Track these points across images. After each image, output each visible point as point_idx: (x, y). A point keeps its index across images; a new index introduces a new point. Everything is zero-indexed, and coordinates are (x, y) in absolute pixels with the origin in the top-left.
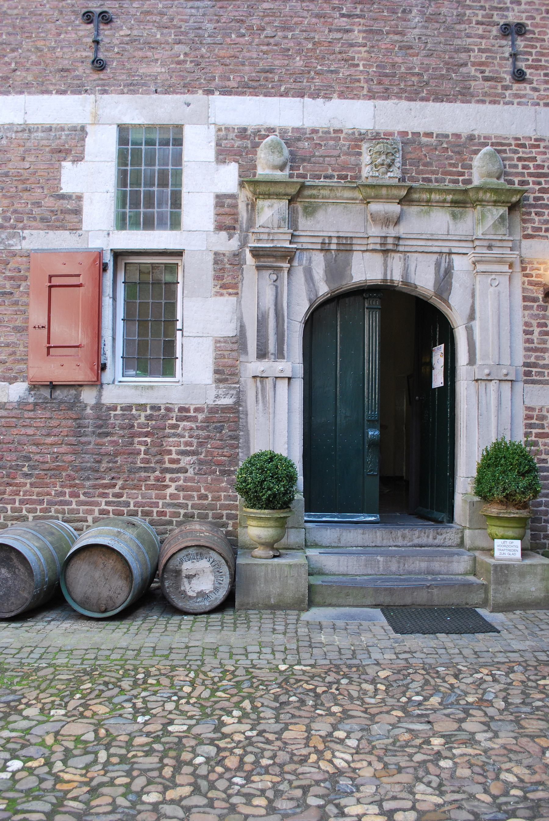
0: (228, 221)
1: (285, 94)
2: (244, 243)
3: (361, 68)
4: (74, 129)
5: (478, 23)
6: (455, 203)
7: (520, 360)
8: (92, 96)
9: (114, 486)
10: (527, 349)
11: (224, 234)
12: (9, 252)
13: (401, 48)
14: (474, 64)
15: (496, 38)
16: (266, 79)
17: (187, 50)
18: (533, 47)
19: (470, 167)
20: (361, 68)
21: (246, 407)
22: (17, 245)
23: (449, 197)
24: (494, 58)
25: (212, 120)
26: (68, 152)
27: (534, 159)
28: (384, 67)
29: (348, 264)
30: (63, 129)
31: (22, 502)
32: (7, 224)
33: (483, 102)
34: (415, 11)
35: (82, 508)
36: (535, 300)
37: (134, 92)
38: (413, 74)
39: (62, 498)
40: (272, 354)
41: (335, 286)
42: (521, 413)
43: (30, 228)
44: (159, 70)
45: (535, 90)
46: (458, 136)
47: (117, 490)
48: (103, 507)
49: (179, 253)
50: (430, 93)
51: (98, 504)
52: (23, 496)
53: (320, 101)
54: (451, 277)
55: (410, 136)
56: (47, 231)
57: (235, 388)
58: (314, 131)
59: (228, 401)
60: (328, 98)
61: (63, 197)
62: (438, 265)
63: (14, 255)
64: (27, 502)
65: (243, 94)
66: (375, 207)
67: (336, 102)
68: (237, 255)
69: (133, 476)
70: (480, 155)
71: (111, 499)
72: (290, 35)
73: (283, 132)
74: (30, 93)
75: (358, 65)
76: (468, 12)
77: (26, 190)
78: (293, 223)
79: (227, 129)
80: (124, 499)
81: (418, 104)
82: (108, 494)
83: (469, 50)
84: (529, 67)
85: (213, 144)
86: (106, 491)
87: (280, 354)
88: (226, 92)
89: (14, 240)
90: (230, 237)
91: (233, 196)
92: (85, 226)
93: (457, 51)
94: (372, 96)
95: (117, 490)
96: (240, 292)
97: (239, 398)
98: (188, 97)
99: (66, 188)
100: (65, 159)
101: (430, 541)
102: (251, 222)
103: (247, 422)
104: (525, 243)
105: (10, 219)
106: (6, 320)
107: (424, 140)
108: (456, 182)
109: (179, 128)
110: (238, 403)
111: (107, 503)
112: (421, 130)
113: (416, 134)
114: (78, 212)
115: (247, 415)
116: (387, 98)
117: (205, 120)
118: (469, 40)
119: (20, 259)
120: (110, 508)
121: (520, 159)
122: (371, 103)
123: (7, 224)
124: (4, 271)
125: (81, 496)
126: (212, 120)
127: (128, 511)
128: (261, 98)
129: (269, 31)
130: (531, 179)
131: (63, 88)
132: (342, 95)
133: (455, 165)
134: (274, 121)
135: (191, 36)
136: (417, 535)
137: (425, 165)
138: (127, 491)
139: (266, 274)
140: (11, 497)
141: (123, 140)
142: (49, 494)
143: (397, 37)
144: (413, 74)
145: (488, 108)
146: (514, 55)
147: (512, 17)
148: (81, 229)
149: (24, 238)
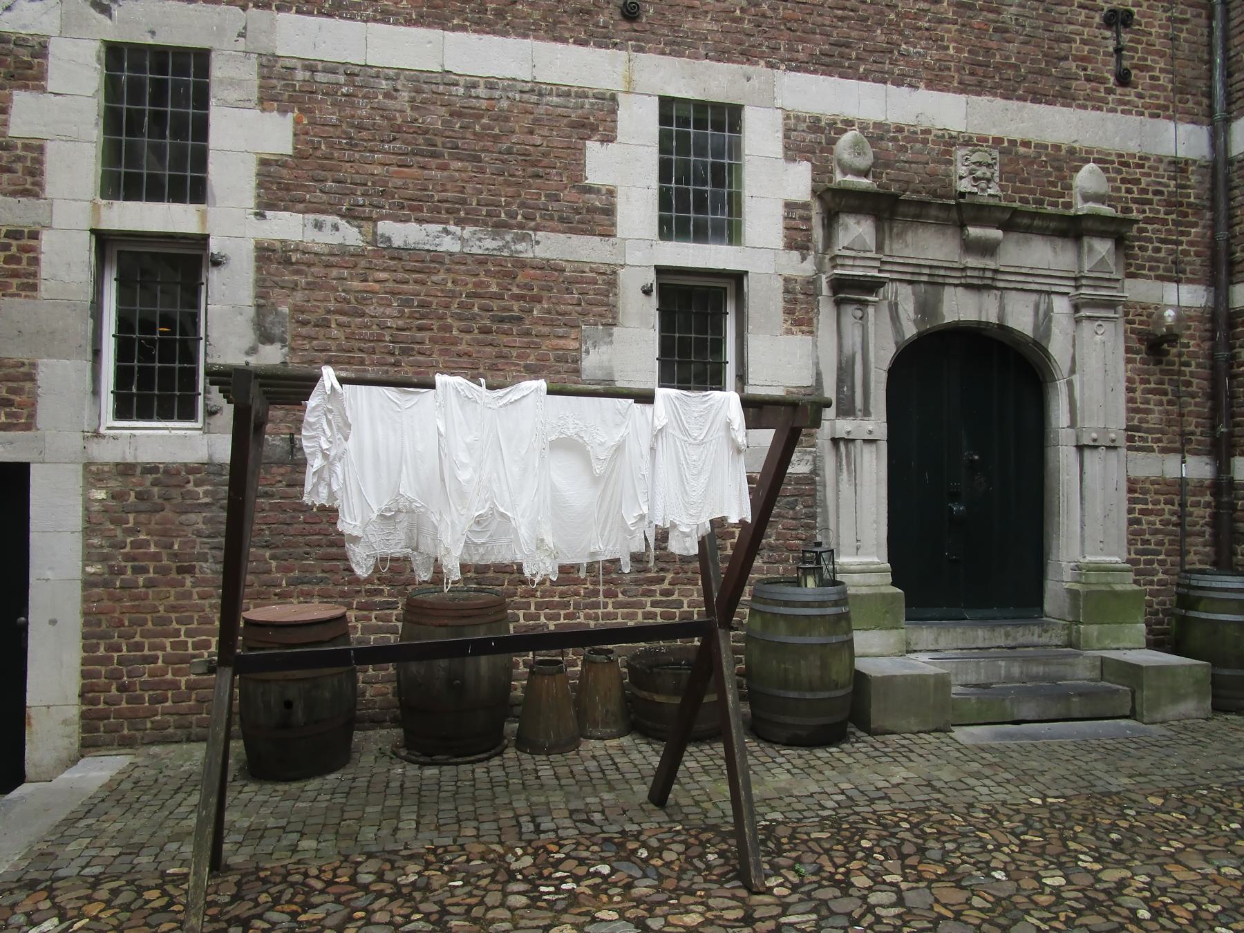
0: (799, 238)
1: (862, 78)
2: (820, 270)
3: (951, 52)
4: (600, 96)
8: (624, 53)
9: (662, 580)
10: (1129, 410)
11: (795, 255)
12: (516, 261)
13: (996, 30)
14: (1076, 59)
16: (842, 56)
18: (1139, 42)
19: (1070, 188)
20: (951, 52)
21: (824, 476)
22: (525, 251)
23: (1053, 225)
24: (1097, 53)
26: (594, 129)
27: (1138, 182)
28: (977, 54)
29: (939, 301)
31: (539, 606)
32: (513, 222)
33: (1085, 107)
35: (620, 611)
37: (680, 54)
39: (594, 599)
40: (860, 410)
41: (922, 329)
43: (544, 229)
44: (709, 27)
45: (1140, 96)
46: (1057, 147)
47: (666, 585)
48: (649, 609)
50: (1027, 91)
51: (642, 605)
52: (541, 597)
53: (905, 90)
54: (1050, 321)
55: (1006, 144)
56: (568, 235)
57: (811, 452)
58: (900, 129)
61: (589, 190)
62: (1037, 307)
63: (522, 264)
64: (549, 605)
66: (974, 231)
68: (812, 282)
69: (686, 567)
71: (659, 598)
73: (863, 127)
74: (536, 38)
75: (947, 48)
77: (538, 176)
79: (797, 118)
80: (675, 597)
81: (1014, 104)
82: (655, 591)
84: (1136, 67)
85: (780, 135)
86: (653, 588)
87: (867, 413)
88: (799, 67)
89: (524, 244)
90: (804, 259)
91: (806, 206)
92: (621, 231)
93: (1058, 40)
94: (963, 89)
95: (666, 585)
96: (815, 330)
97: (815, 464)
99: (593, 177)
100: (589, 138)
101: (1035, 639)
103: (825, 495)
104: (1128, 283)
105: (517, 214)
106: (515, 354)
107: (1022, 150)
108: (1055, 205)
110: (814, 472)
111: (654, 604)
112: (1017, 137)
113: (1013, 142)
114: (609, 211)
115: (825, 486)
117: (768, 102)
118: (1071, 27)
119: (532, 272)
120: (658, 610)
121: (1123, 181)
122: (963, 97)
123: (513, 222)
124: (509, 287)
125: (620, 595)
126: (778, 103)
127: (681, 613)
128: (836, 79)
130: (1134, 206)
131: (583, 36)
132: (930, 85)
133: (1054, 184)
134: (851, 112)
136: (1021, 633)
137: (1024, 181)
138: (678, 586)
140: (524, 600)
141: (664, 119)
142: (578, 594)
143: (991, 16)
145: (1090, 115)
146: (1118, 51)
148: (615, 236)
149: (538, 243)
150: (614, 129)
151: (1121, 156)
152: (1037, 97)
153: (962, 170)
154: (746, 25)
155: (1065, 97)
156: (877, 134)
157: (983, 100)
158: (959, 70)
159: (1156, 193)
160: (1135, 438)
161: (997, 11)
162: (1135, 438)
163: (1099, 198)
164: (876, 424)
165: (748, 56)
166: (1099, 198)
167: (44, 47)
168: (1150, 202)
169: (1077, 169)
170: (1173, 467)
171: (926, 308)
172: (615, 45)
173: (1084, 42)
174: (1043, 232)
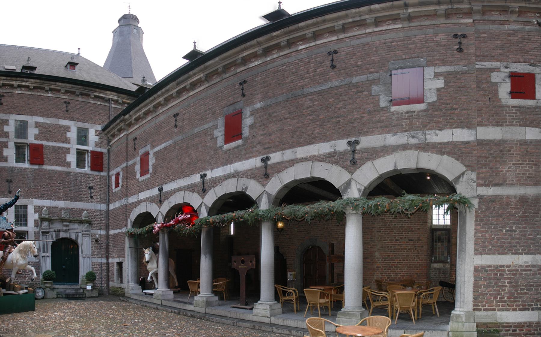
2: (40, 230)
6: (79, 223)
7: (91, 253)
29: (59, 234)
36: (93, 241)
42: (91, 263)
46: (80, 209)
49: (28, 231)
58: (53, 207)
59: (37, 261)
60: (55, 200)
62: (76, 234)
66: (64, 223)
67: (57, 201)
68: (39, 232)
73: (47, 207)
78: (49, 227)
91: (37, 220)
98: (28, 199)
102: (41, 226)
104: (92, 230)
109: (27, 206)
129: (44, 186)
139: (44, 236)
147: (91, 185)
153: (63, 214)
155: (81, 201)
156: (49, 208)
157: (67, 202)
160: (93, 255)
162: (93, 255)
163: (85, 217)
164: (49, 254)
166: (85, 217)
170: (100, 260)
171: (57, 235)
174: (77, 223)
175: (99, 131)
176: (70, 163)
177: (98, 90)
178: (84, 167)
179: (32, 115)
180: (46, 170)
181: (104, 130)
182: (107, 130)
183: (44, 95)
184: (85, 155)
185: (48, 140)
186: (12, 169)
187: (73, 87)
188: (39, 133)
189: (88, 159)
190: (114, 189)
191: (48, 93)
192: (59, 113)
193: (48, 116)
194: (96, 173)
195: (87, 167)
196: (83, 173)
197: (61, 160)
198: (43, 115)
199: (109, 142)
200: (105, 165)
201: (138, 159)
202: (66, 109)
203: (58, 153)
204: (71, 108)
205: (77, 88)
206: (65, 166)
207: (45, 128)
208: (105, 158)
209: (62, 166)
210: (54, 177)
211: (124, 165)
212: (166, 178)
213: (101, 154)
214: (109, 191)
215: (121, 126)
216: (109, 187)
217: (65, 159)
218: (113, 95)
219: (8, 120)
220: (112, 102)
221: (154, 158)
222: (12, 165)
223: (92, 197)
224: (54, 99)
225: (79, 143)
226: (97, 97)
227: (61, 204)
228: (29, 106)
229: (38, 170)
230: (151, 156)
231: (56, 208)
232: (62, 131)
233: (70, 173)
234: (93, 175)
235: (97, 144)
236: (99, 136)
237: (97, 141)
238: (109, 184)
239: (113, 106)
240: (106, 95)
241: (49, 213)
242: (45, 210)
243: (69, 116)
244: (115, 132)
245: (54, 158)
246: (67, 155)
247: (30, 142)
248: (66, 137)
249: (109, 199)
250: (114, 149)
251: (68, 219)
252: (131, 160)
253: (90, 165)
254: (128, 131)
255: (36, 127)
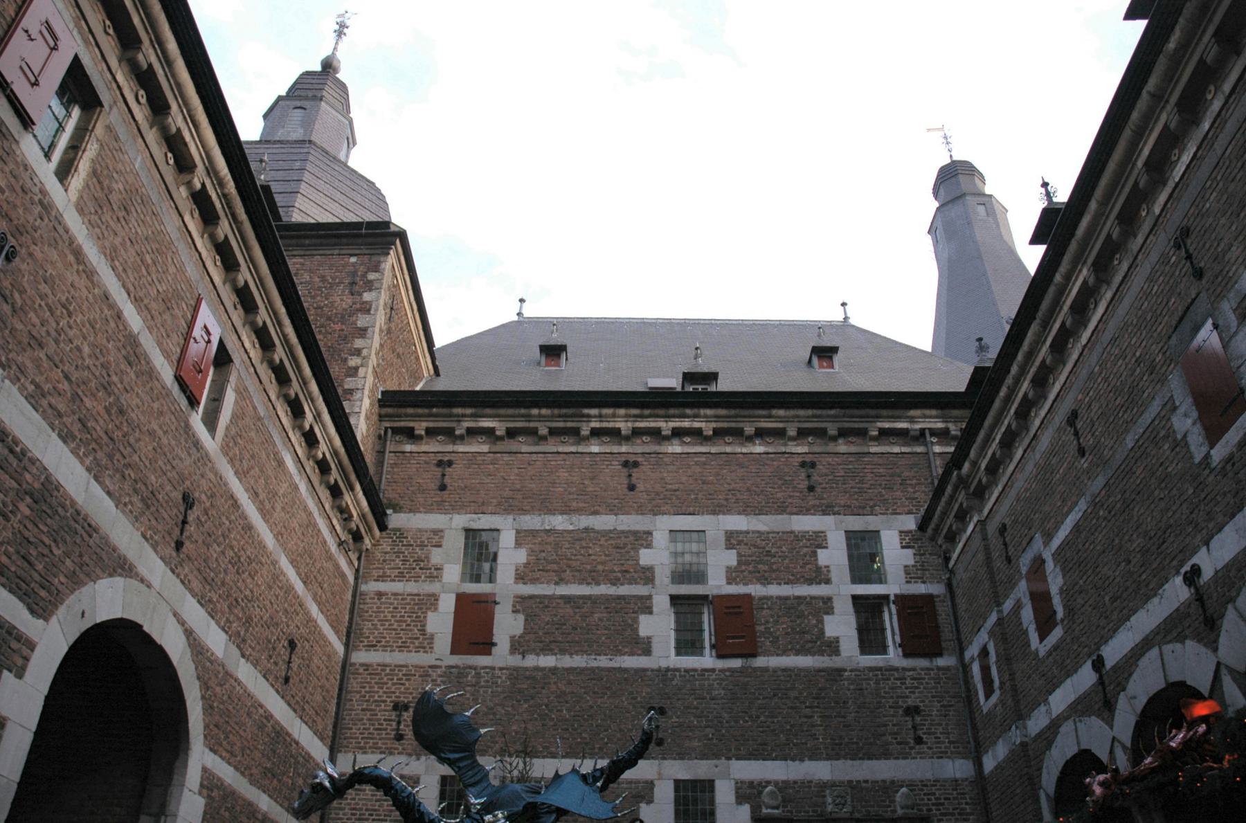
4: (646, 782)
5: (890, 707)
13: (844, 726)
14: (890, 734)
15: (902, 716)
17: (713, 731)
18: (926, 720)
19: (894, 801)
25: (732, 776)
27: (934, 794)
30: (639, 782)
33: (897, 758)
34: (850, 702)
37: (682, 759)
38: (853, 743)
45: (930, 748)
46: (884, 781)
53: (797, 762)
58: (795, 782)
60: (802, 760)
65: (749, 759)
70: (899, 794)
72: (776, 720)
73: (776, 783)
76: (883, 700)
81: (857, 762)
83: (886, 725)
84: (925, 734)
94: (829, 758)
107: (864, 785)
112: (861, 778)
113: (858, 782)
116: (838, 759)
117: (726, 775)
121: (925, 794)
122: (828, 763)
126: (732, 776)
128: (761, 762)
129: (762, 718)
130: (934, 808)
132: (811, 759)
133: (884, 801)
135: (716, 722)
141: (677, 790)
144: (853, 743)
145: (902, 762)
146: (914, 727)
147: (910, 702)
150: (652, 797)
151: (922, 781)
152: (870, 757)
153: (829, 800)
154: (715, 741)
155: (886, 755)
156: (783, 787)
157: (840, 762)
158: (826, 748)
159: (945, 799)
161: (844, 717)
165: (717, 756)
167: (418, 779)
168: (942, 804)
169: (897, 791)
172: (653, 758)
173: (894, 725)
175: (910, 532)
176: (837, 640)
177: (884, 412)
178: (883, 649)
179: (714, 513)
180: (766, 669)
181: (922, 527)
182: (932, 525)
183: (744, 450)
184: (881, 612)
185: (765, 581)
186: (665, 674)
187: (814, 416)
188: (739, 563)
189: (890, 620)
190: (986, 704)
191: (755, 444)
192: (790, 497)
193: (759, 511)
194: (922, 663)
195: (891, 649)
196: (880, 669)
197: (808, 637)
198: (747, 509)
199: (947, 559)
200: (947, 633)
201: (1023, 584)
202: (807, 483)
203: (799, 617)
204: (820, 480)
205: (828, 416)
206: (821, 653)
207: (755, 546)
208: (943, 611)
209: (813, 654)
210: (793, 688)
211: (993, 618)
212: (1103, 622)
213: (929, 599)
214: (971, 712)
215: (959, 501)
216: (969, 699)
217: (822, 632)
218: (931, 417)
219: (649, 533)
220: (934, 440)
221: (1058, 570)
222: (664, 664)
223: (919, 740)
224: (773, 460)
225: (856, 579)
226: (884, 433)
227: (820, 770)
228: (705, 487)
229: (741, 671)
230: (1050, 565)
231: (806, 784)
232: (805, 550)
233: (840, 671)
234: (914, 669)
235: (911, 574)
236: (913, 547)
237: (911, 562)
238: (968, 690)
239: (937, 449)
240: (912, 420)
241: (786, 801)
242: (772, 793)
243: (817, 502)
244: (951, 526)
245: (787, 634)
246: (826, 617)
247: (715, 592)
248: (816, 565)
249: (976, 740)
250: (961, 575)
251: (847, 815)
252: (1007, 596)
253: (898, 639)
254: (981, 511)
255: (729, 546)
